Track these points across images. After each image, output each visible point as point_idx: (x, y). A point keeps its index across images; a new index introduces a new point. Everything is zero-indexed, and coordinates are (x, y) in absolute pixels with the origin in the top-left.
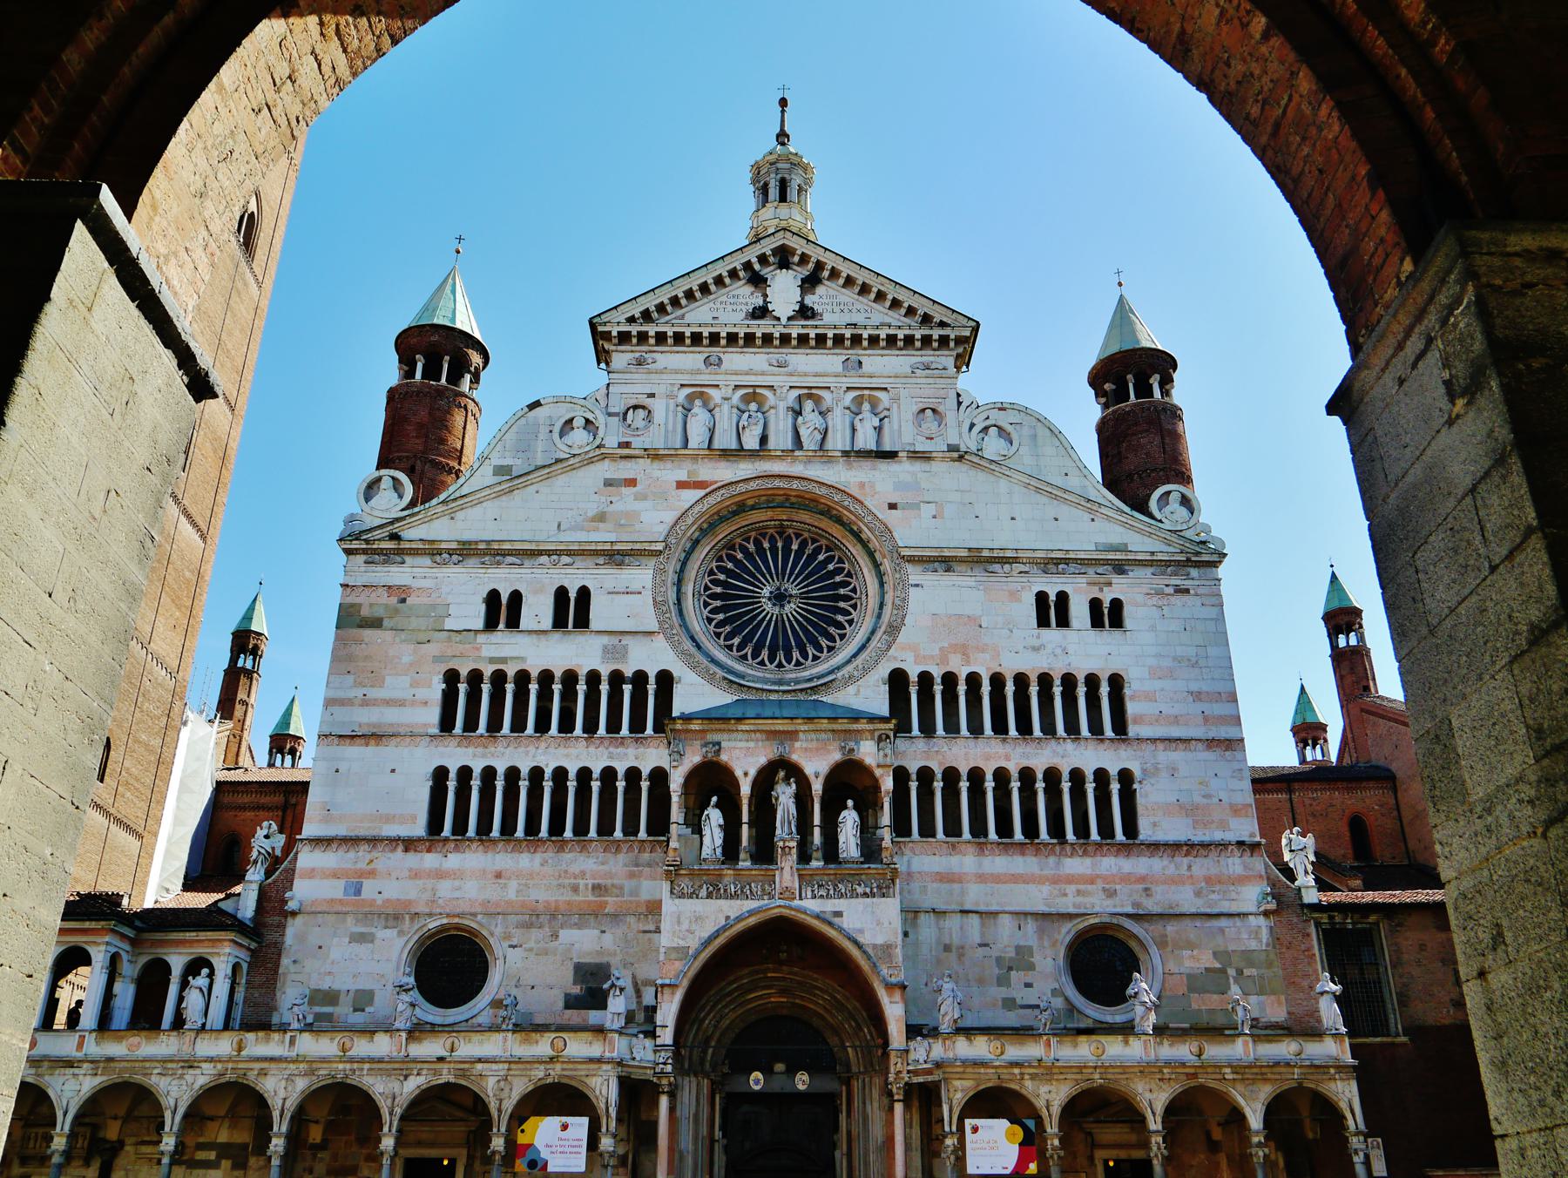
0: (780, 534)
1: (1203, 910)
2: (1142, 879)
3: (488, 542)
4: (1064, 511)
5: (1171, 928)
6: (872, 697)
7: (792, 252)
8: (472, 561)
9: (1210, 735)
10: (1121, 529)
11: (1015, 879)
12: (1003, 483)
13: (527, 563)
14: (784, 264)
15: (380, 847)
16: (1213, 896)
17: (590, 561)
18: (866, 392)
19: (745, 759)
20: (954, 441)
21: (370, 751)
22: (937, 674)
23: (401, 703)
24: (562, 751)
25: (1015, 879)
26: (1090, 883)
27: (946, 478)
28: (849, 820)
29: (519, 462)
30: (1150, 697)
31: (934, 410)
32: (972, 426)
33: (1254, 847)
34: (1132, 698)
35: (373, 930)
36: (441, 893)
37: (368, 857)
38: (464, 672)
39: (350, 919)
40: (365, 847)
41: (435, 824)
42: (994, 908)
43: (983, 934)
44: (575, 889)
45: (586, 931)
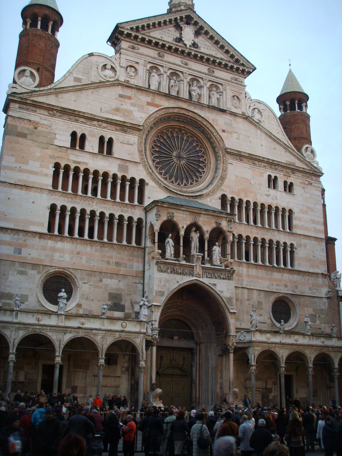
0: (180, 131)
1: (310, 295)
2: (295, 282)
3: (75, 111)
4: (278, 147)
5: (302, 300)
6: (215, 203)
7: (192, 19)
8: (66, 117)
9: (316, 236)
10: (293, 157)
11: (258, 277)
12: (259, 131)
13: (89, 122)
14: (188, 23)
15: (30, 235)
16: (314, 291)
17: (113, 127)
18: (215, 84)
20: (244, 111)
21: (23, 192)
22: (237, 198)
23: (35, 173)
24: (103, 205)
25: (258, 277)
26: (280, 283)
27: (241, 125)
28: (217, 250)
29: (84, 78)
30: (300, 219)
31: (237, 97)
32: (250, 107)
33: (326, 275)
34: (295, 219)
35: (27, 270)
36: (55, 258)
37: (24, 238)
38: (63, 165)
39: (17, 264)
40: (21, 234)
41: (51, 228)
42: (252, 287)
43: (248, 296)
44: (108, 263)
45: (113, 280)
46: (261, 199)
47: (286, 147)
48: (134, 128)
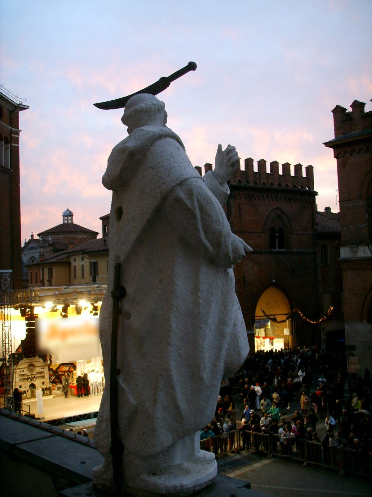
6: (35, 373)
19: (30, 377)
27: (38, 362)
46: (41, 371)
47: (43, 363)
48: (26, 368)
